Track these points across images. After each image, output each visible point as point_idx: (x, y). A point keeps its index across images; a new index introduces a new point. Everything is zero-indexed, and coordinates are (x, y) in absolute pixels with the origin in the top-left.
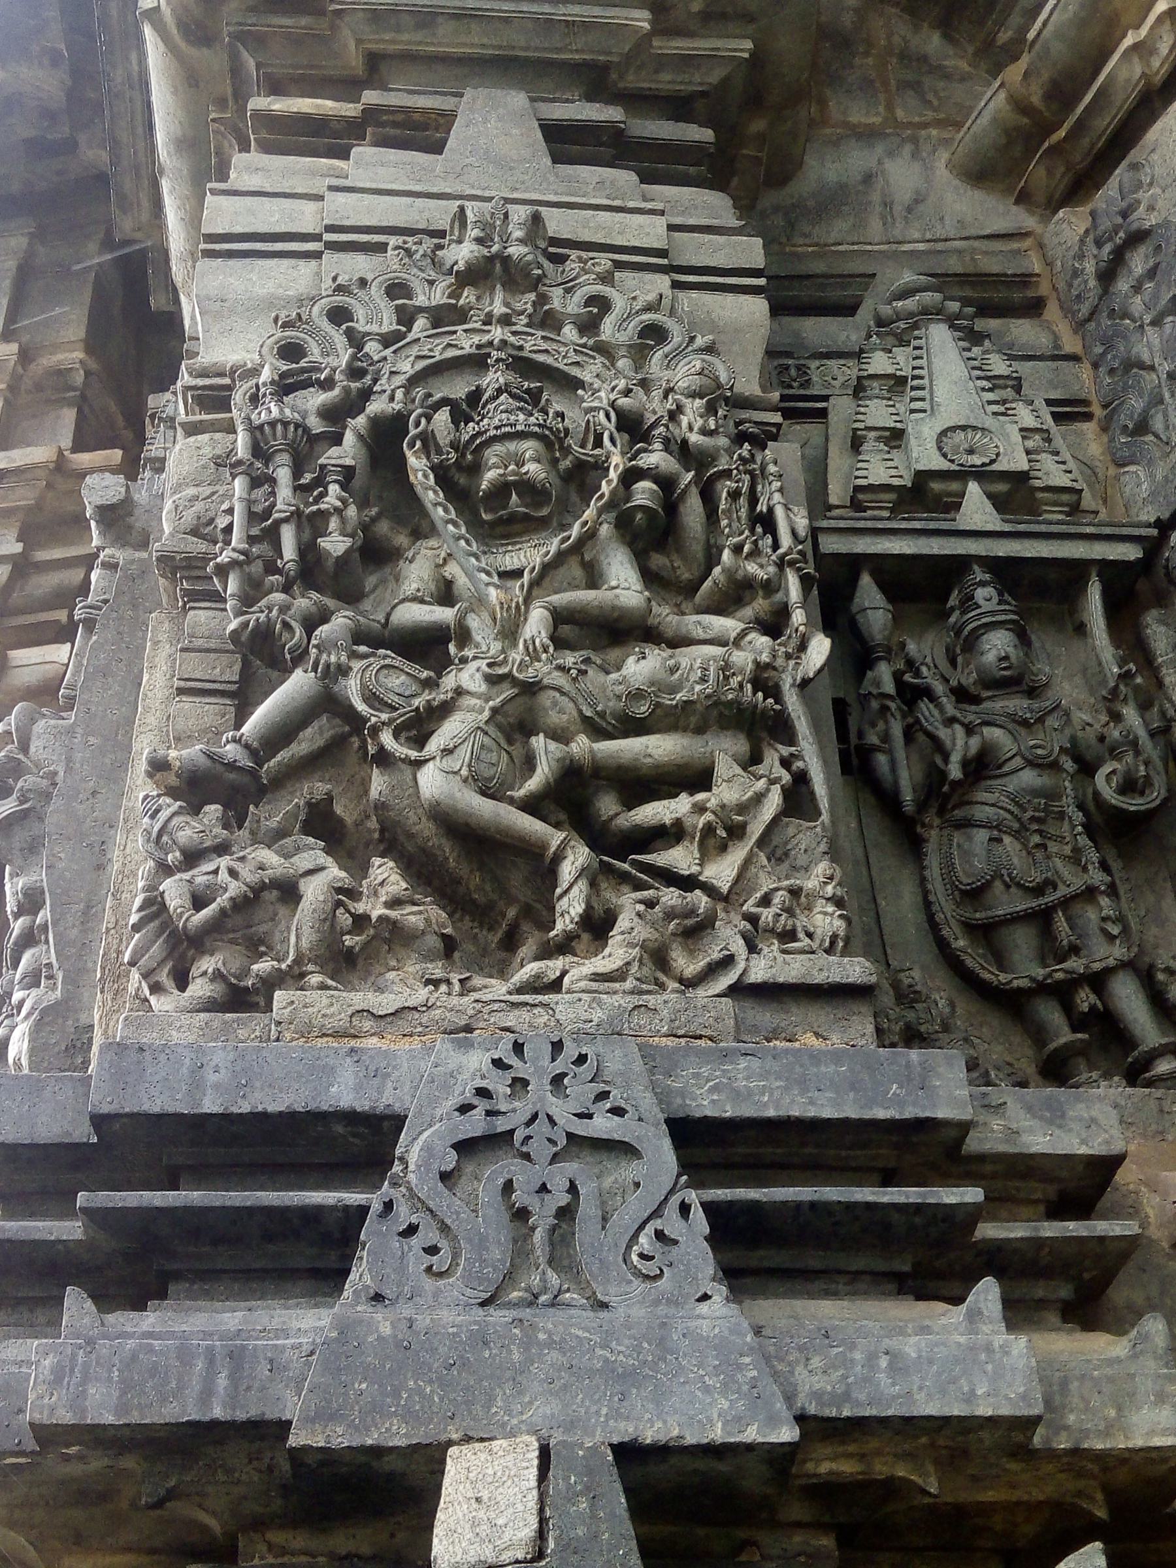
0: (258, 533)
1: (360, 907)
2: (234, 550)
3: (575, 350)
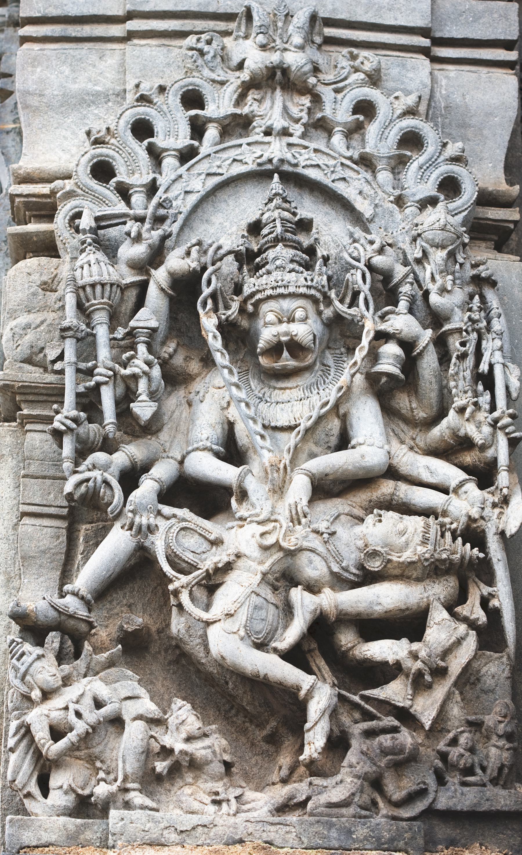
0: (83, 390)
1: (168, 740)
2: (66, 417)
3: (342, 164)
